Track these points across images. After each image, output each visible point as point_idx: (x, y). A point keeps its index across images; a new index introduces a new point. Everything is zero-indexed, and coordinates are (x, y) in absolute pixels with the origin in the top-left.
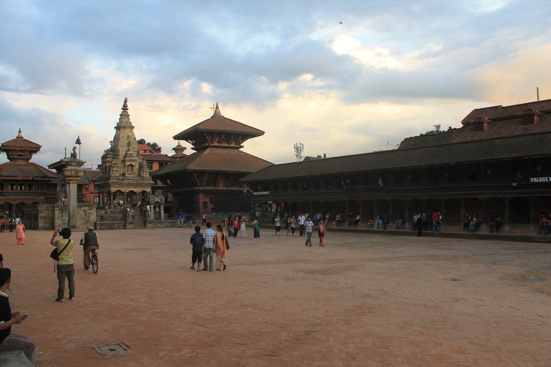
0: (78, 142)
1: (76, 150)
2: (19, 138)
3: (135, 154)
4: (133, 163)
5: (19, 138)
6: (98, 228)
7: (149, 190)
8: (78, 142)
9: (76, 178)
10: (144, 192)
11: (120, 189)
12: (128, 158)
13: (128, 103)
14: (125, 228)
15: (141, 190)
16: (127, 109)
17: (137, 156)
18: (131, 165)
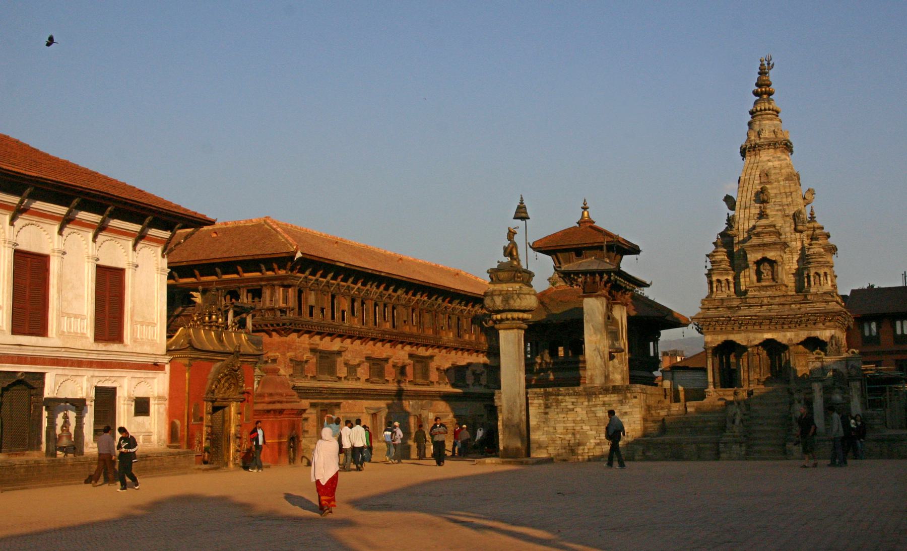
0: (521, 214)
1: (516, 238)
2: (586, 224)
3: (787, 228)
4: (771, 255)
5: (586, 224)
6: (637, 458)
7: (825, 334)
8: (521, 214)
9: (509, 316)
10: (813, 344)
11: (732, 337)
12: (755, 241)
13: (772, 75)
14: (717, 456)
15: (803, 335)
16: (770, 94)
17: (796, 230)
18: (765, 260)
